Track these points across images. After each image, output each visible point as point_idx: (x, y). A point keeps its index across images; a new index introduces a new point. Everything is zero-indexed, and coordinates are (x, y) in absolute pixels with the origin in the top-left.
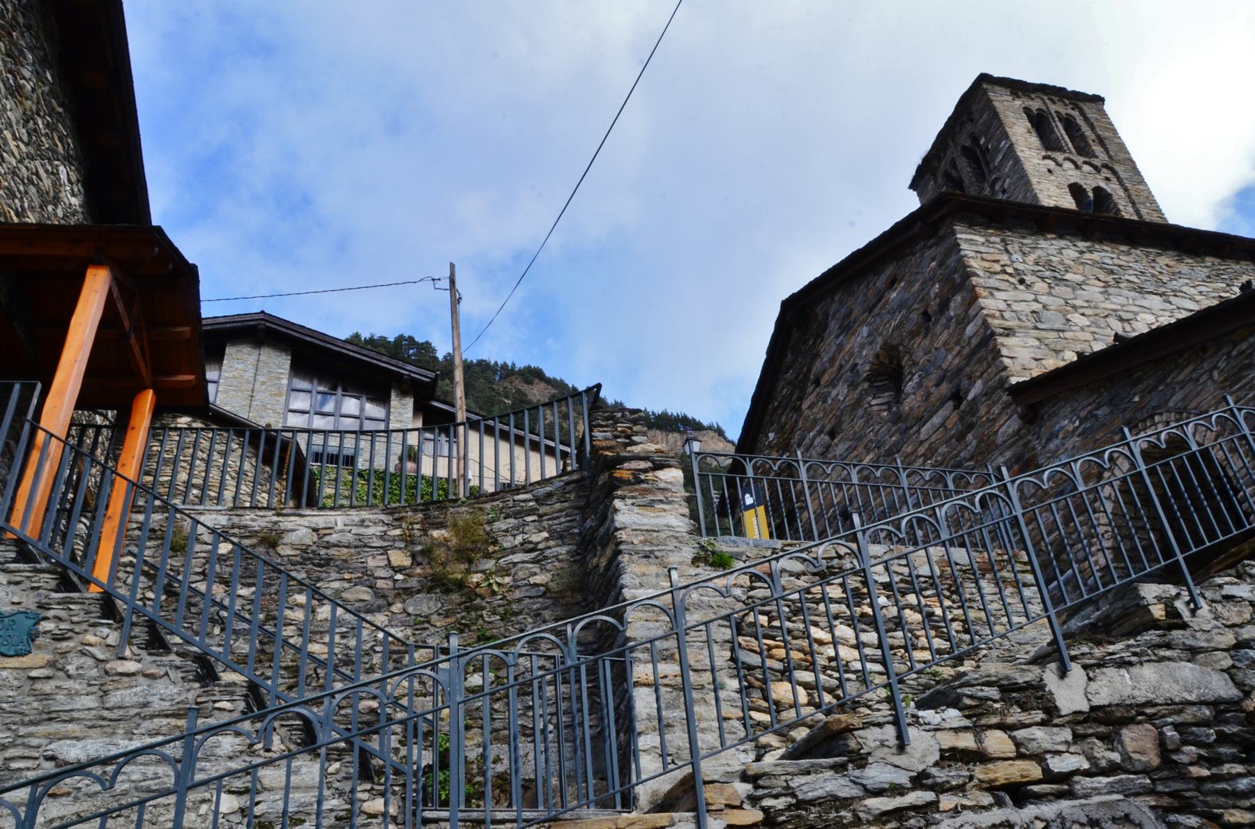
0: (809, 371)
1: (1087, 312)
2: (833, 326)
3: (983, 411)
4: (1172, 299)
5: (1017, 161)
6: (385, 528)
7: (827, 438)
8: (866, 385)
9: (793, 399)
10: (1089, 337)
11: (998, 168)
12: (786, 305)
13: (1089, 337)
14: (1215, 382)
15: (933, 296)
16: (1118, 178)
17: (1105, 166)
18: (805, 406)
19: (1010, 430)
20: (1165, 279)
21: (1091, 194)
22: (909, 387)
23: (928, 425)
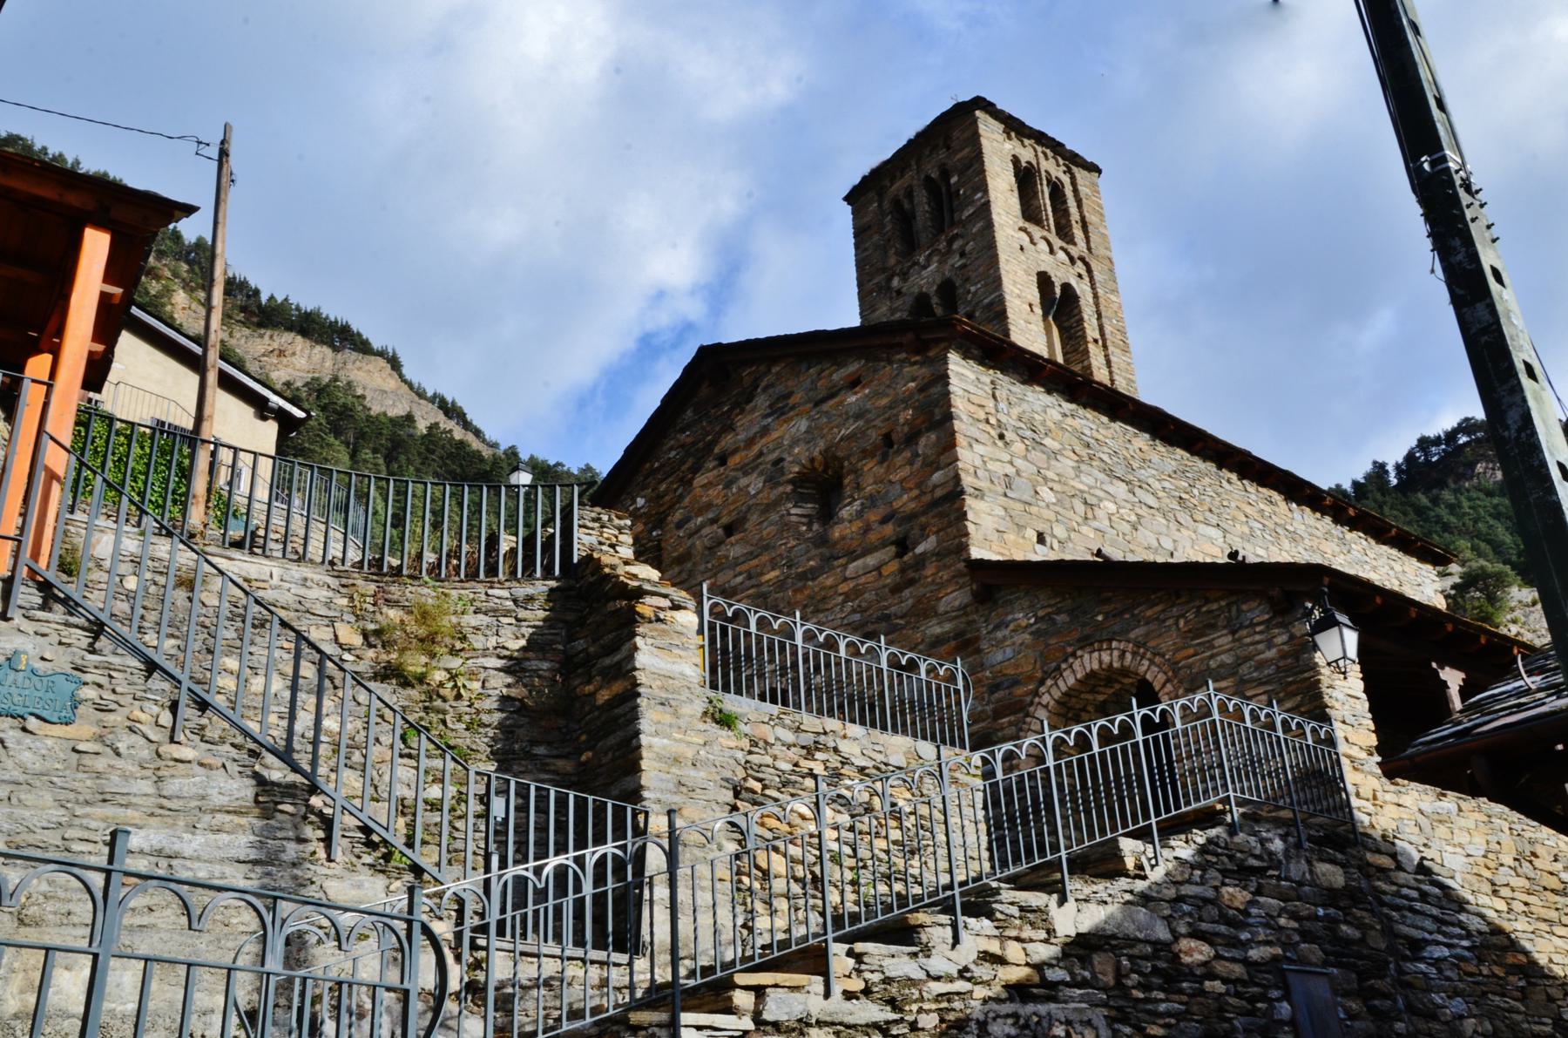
0: (715, 442)
1: (1057, 487)
2: (762, 402)
3: (929, 571)
4: (1137, 490)
5: (990, 225)
6: (331, 594)
7: (720, 531)
8: (789, 488)
9: (683, 468)
10: (1052, 516)
11: (963, 224)
12: (705, 353)
13: (1052, 516)
14: (1178, 629)
15: (902, 421)
17: (1082, 259)
18: (700, 480)
19: (957, 603)
20: (1135, 465)
21: (1058, 291)
22: (845, 513)
23: (859, 563)
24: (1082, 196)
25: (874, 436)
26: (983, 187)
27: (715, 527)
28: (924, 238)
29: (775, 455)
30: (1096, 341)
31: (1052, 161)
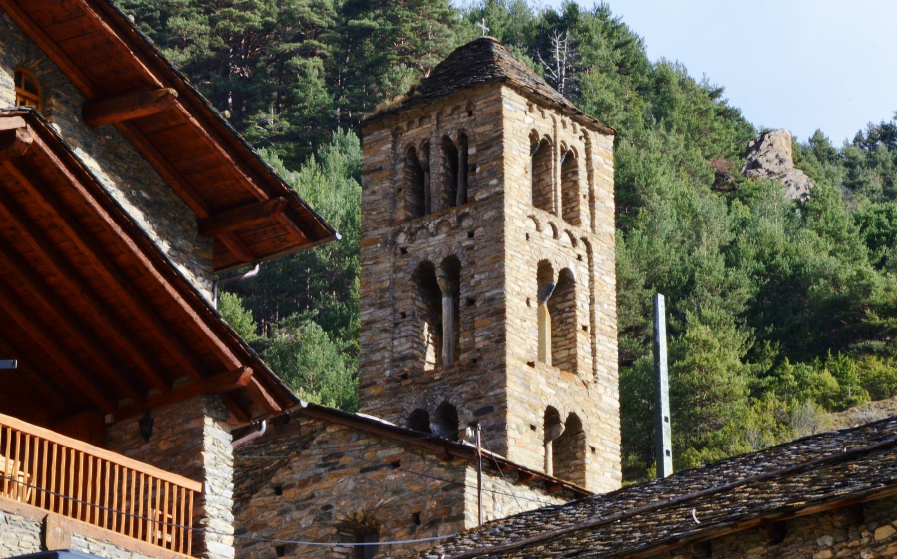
0: (271, 473)
2: (316, 454)
5: (500, 218)
8: (335, 531)
15: (428, 507)
16: (590, 259)
17: (584, 240)
21: (556, 278)
24: (594, 166)
25: (407, 513)
26: (498, 173)
27: (268, 544)
28: (436, 203)
29: (325, 501)
30: (585, 328)
31: (569, 127)
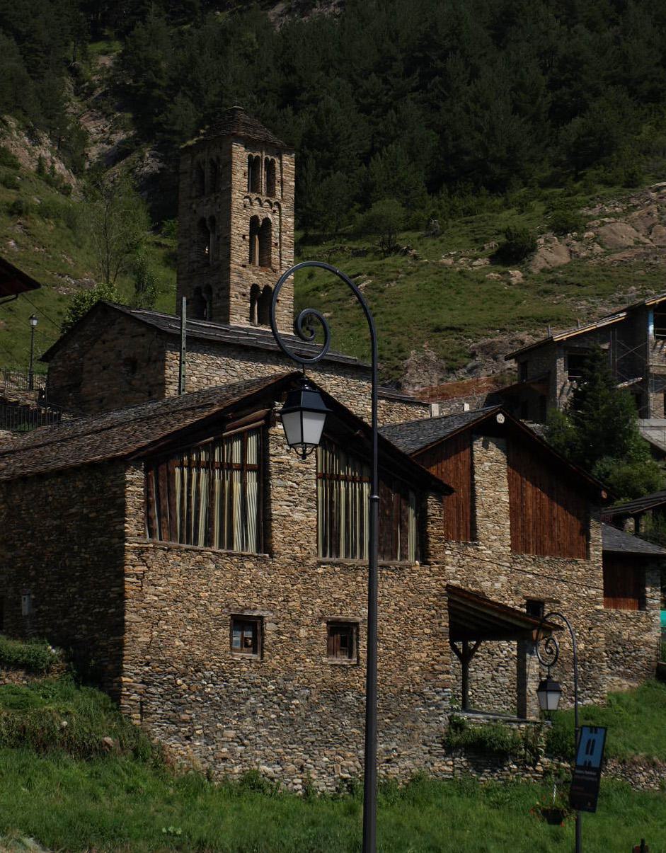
21: (261, 223)
